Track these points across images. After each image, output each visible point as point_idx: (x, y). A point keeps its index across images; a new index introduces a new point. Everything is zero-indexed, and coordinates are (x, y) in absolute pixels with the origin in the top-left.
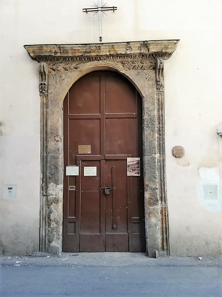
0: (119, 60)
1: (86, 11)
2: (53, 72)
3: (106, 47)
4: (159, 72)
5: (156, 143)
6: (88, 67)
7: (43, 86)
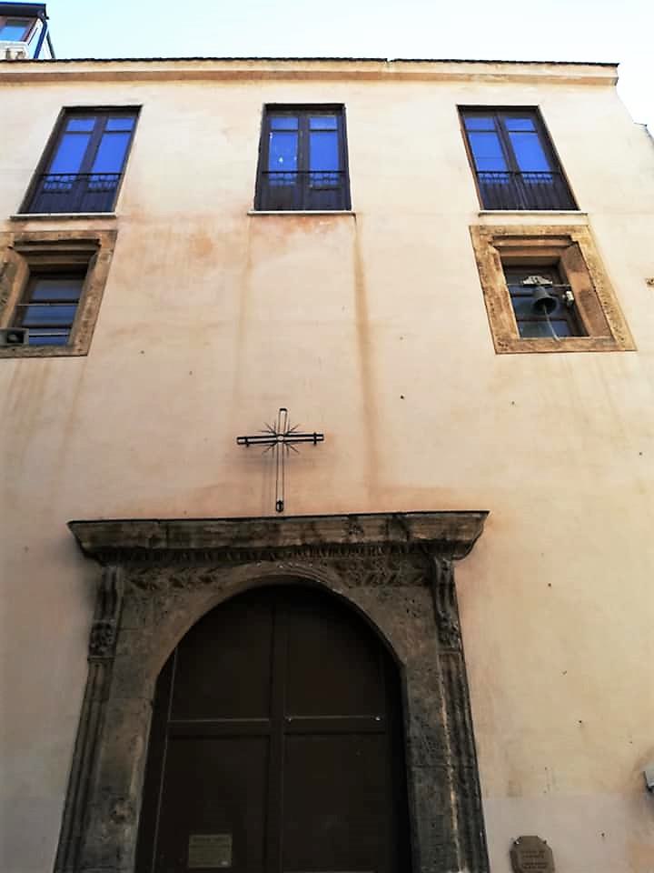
0: (327, 558)
1: (246, 441)
2: (139, 593)
3: (294, 527)
4: (442, 593)
5: (455, 825)
6: (242, 575)
7: (103, 632)
